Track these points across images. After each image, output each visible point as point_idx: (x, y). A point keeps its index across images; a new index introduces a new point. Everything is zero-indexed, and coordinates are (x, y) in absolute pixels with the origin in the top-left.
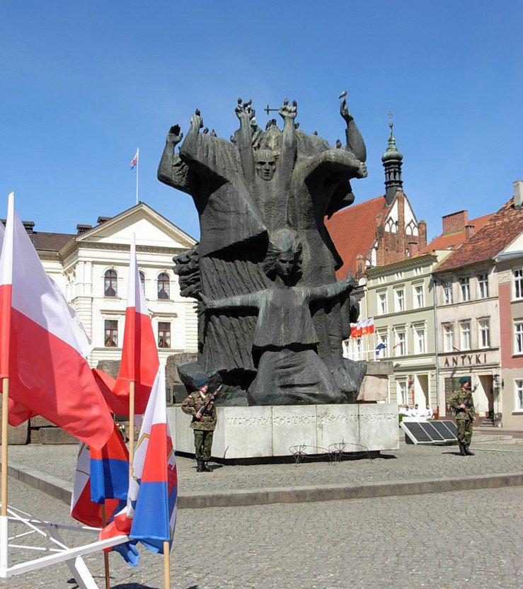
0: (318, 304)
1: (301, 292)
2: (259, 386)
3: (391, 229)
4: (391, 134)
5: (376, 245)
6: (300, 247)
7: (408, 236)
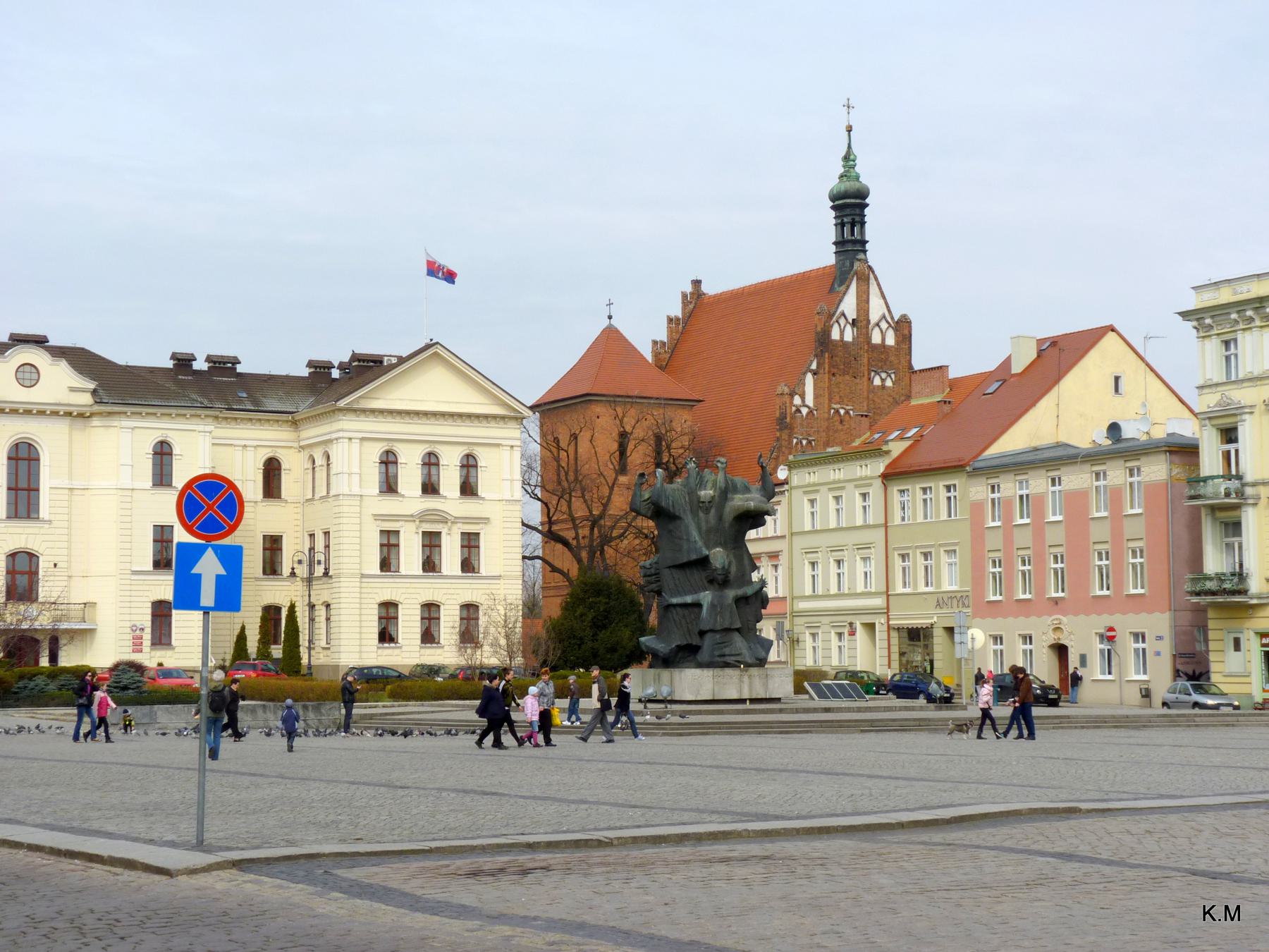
0: (741, 601)
1: (731, 594)
2: (704, 656)
3: (842, 333)
4: (849, 147)
5: (814, 366)
6: (730, 564)
7: (875, 347)
